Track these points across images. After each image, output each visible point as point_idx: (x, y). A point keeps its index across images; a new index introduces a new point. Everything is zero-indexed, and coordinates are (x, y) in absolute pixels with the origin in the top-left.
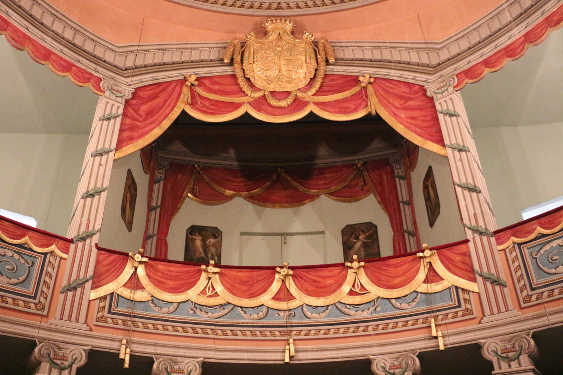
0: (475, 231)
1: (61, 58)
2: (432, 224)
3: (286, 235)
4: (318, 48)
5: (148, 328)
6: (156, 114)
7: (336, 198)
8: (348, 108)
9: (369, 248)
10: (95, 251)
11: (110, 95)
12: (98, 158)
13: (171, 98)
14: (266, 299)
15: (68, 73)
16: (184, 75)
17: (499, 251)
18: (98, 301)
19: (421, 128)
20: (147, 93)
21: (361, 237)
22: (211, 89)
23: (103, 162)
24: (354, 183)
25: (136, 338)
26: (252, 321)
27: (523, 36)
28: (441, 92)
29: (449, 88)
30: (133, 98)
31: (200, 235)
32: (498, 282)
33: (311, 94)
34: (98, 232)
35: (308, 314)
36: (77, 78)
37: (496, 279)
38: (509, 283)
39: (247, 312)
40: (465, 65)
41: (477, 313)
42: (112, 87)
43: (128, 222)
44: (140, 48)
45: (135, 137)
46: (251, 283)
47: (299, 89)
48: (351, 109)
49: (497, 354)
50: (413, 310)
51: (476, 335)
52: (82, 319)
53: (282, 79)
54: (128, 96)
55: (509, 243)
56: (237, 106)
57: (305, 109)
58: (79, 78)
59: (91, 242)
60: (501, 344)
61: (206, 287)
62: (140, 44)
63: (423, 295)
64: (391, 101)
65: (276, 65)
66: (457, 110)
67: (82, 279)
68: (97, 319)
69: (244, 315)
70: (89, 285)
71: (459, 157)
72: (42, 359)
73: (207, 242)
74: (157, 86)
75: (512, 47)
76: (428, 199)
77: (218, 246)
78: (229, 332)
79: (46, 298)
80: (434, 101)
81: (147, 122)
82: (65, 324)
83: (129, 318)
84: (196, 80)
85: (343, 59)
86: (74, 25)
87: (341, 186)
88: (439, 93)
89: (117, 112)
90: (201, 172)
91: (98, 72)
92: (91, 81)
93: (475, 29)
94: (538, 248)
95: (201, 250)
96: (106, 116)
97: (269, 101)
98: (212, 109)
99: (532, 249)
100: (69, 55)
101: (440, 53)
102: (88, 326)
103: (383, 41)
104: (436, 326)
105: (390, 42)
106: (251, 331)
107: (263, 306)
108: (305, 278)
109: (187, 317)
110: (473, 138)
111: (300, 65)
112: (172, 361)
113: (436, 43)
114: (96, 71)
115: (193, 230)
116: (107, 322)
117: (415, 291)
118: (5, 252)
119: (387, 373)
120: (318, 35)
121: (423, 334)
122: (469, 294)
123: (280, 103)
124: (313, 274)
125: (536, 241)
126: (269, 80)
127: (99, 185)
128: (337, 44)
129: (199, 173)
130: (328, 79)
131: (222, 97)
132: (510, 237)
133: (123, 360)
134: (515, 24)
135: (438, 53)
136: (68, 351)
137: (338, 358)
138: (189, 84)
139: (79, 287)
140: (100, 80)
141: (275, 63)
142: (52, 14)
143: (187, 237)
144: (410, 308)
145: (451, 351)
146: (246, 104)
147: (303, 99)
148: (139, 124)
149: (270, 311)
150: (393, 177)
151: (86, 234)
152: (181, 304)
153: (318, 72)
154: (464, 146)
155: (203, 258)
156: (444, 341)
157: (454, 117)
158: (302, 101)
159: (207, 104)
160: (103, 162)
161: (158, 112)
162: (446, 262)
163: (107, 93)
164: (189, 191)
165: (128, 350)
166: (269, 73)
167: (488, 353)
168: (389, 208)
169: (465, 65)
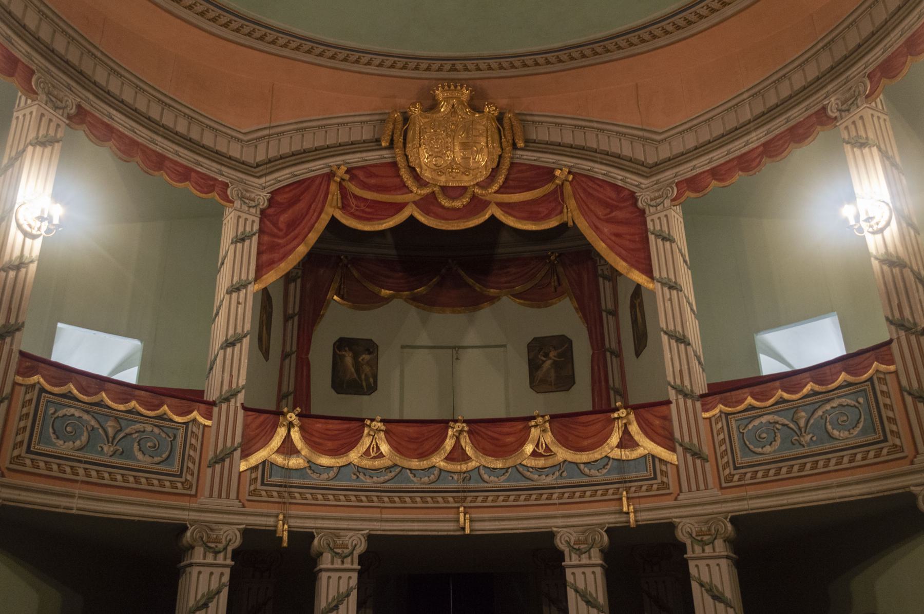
0: (680, 391)
1: (176, 163)
2: (638, 354)
5: (306, 499)
6: (299, 224)
7: (521, 301)
10: (241, 413)
11: (241, 208)
12: (234, 295)
14: (438, 460)
15: (187, 183)
16: (330, 166)
18: (249, 472)
20: (286, 196)
21: (552, 354)
26: (423, 486)
27: (761, 145)
28: (655, 204)
29: (665, 201)
30: (270, 206)
31: (350, 350)
32: (699, 456)
34: (243, 388)
35: (486, 477)
36: (198, 188)
37: (697, 451)
38: (712, 458)
39: (417, 475)
40: (688, 172)
41: (673, 488)
42: (242, 193)
47: (478, 183)
48: (542, 215)
51: (671, 513)
52: (233, 494)
53: (456, 169)
54: (263, 204)
55: (716, 411)
56: (400, 207)
57: (485, 212)
58: (201, 187)
59: (236, 402)
60: (696, 525)
63: (615, 461)
64: (592, 207)
65: (448, 151)
67: (230, 448)
68: (249, 492)
69: (413, 479)
70: (237, 454)
71: (668, 297)
73: (360, 359)
76: (634, 321)
77: (374, 364)
79: (192, 474)
81: (289, 237)
82: (215, 503)
84: (347, 172)
86: (187, 111)
87: (528, 286)
88: (652, 206)
90: (349, 266)
91: (224, 175)
92: (217, 189)
93: (705, 121)
95: (353, 370)
98: (369, 213)
99: (740, 422)
100: (186, 157)
101: (659, 149)
102: (240, 502)
103: (588, 118)
104: (628, 498)
106: (421, 497)
109: (349, 483)
110: (689, 268)
112: (335, 535)
113: (655, 133)
115: (342, 344)
116: (261, 496)
118: (144, 427)
119: (571, 548)
120: (503, 102)
121: (613, 507)
122: (666, 466)
123: (453, 204)
125: (746, 413)
126: (439, 170)
127: (239, 330)
128: (529, 118)
129: (347, 266)
132: (718, 404)
133: (281, 538)
134: (754, 125)
135: (657, 148)
136: (222, 532)
138: (338, 180)
140: (226, 185)
141: (447, 147)
144: (601, 476)
145: (642, 528)
146: (411, 204)
148: (280, 241)
151: (230, 394)
152: (342, 468)
153: (502, 161)
154: (676, 283)
157: (668, 242)
158: (482, 200)
161: (302, 222)
162: (644, 426)
163: (237, 204)
164: (334, 292)
165: (286, 527)
167: (683, 535)
169: (688, 172)
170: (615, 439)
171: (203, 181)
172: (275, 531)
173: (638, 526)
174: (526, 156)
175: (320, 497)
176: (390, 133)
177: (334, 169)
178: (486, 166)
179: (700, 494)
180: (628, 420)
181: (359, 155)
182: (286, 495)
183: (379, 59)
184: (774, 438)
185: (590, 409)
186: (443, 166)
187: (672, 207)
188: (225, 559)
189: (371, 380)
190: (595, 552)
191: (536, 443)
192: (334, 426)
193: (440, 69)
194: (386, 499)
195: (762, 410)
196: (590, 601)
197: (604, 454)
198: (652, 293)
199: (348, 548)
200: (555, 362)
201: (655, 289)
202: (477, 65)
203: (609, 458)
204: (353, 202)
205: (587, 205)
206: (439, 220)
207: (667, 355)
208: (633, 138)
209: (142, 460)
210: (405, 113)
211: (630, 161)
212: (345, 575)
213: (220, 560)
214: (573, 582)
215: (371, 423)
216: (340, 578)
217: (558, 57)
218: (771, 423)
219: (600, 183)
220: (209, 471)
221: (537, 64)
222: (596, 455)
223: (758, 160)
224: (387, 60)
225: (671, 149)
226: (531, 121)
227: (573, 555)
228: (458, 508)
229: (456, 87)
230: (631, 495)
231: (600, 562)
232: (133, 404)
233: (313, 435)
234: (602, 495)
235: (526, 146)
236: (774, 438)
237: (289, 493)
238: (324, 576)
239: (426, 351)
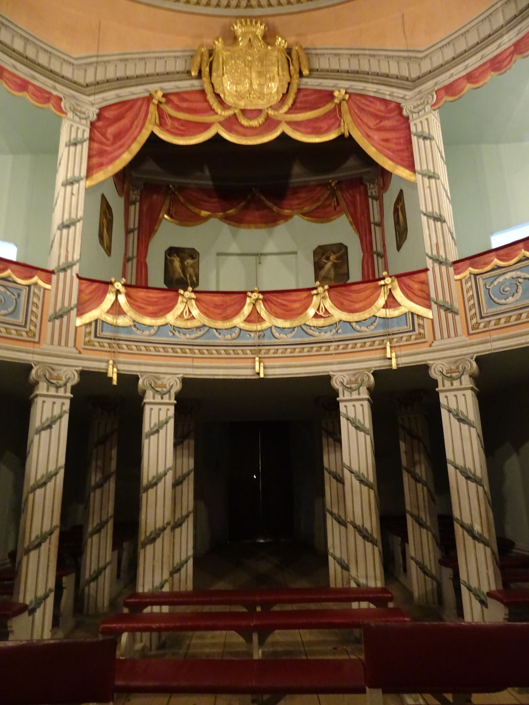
0: (437, 260)
1: (14, 75)
2: (399, 248)
3: (261, 256)
8: (321, 128)
10: (76, 281)
12: (69, 188)
14: (238, 321)
17: (456, 280)
19: (393, 151)
21: (332, 258)
23: (75, 192)
24: (327, 203)
25: (121, 358)
26: (227, 342)
27: (512, 45)
29: (426, 107)
31: (178, 256)
33: (283, 112)
34: (78, 261)
35: (277, 335)
37: (449, 307)
41: (429, 337)
43: (107, 247)
44: (100, 59)
48: (324, 129)
49: (442, 374)
55: (466, 274)
56: (207, 126)
59: (72, 272)
61: (183, 312)
64: (365, 120)
66: (431, 133)
70: (74, 312)
71: (428, 185)
73: (186, 263)
75: (500, 59)
76: (397, 223)
77: (196, 267)
78: (205, 352)
79: (35, 326)
82: (55, 349)
83: (113, 341)
86: (23, 34)
87: (314, 206)
88: (415, 113)
90: (176, 193)
92: (52, 101)
93: (462, 34)
95: (180, 271)
97: (240, 121)
101: (422, 65)
102: (77, 349)
104: (391, 347)
105: (369, 50)
106: (225, 350)
107: (236, 328)
108: (274, 302)
111: (271, 78)
113: (419, 51)
114: (55, 88)
115: (172, 251)
117: (374, 316)
119: (344, 387)
120: (292, 39)
121: (379, 354)
122: (423, 320)
126: (240, 96)
129: (174, 194)
130: (301, 94)
133: (111, 379)
135: (419, 65)
136: (62, 372)
137: (302, 373)
139: (65, 315)
140: (61, 99)
143: (166, 258)
145: (403, 370)
148: (108, 148)
149: (242, 332)
152: (161, 328)
153: (291, 86)
154: (434, 173)
155: (182, 278)
156: (397, 361)
159: (176, 124)
160: (74, 192)
163: (70, 115)
165: (115, 370)
166: (240, 88)
167: (435, 372)
168: (360, 229)
170: (382, 301)
172: (106, 373)
173: (399, 369)
177: (153, 93)
178: (277, 92)
179: (450, 340)
180: (393, 286)
184: (517, 290)
187: (432, 111)
188: (65, 392)
189: (194, 279)
191: (317, 307)
194: (197, 351)
195: (507, 268)
197: (372, 314)
198: (414, 185)
203: (376, 317)
204: (169, 122)
205: (361, 119)
207: (426, 232)
211: (397, 78)
212: (164, 408)
214: (345, 412)
216: (160, 409)
218: (513, 278)
219: (371, 99)
222: (365, 315)
227: (346, 392)
228: (254, 358)
230: (393, 345)
233: (136, 301)
235: (310, 74)
236: (517, 290)
237: (118, 344)
239: (236, 257)
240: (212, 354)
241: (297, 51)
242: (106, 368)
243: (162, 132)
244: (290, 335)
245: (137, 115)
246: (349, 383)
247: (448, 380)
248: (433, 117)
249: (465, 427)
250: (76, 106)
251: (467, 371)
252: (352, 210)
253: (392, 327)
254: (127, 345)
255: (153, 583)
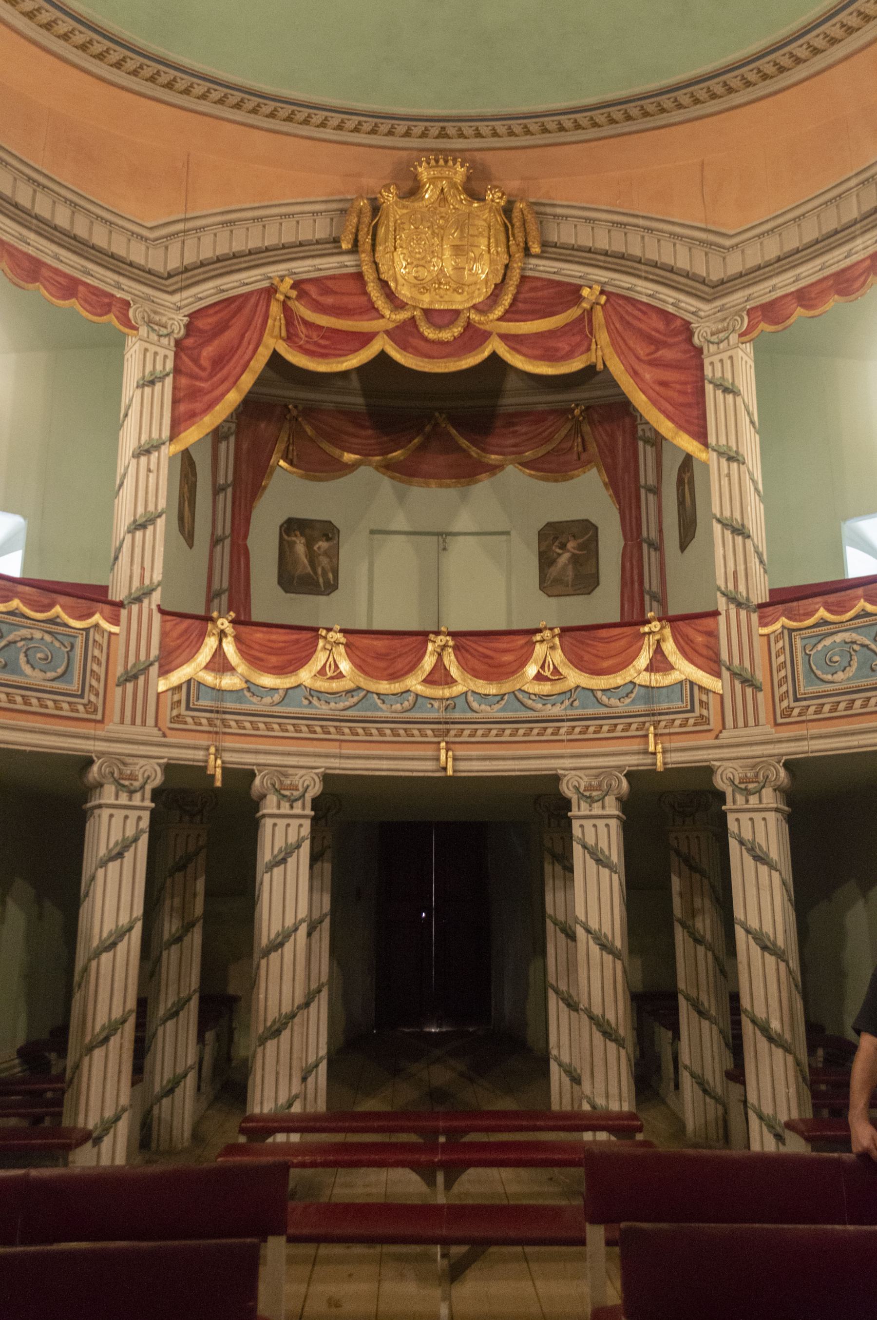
0: (732, 599)
1: (57, 271)
2: (683, 547)
4: (511, 222)
5: (244, 728)
6: (228, 362)
7: (532, 472)
8: (557, 350)
9: (581, 565)
10: (157, 617)
12: (143, 460)
13: (252, 327)
14: (414, 683)
15: (74, 300)
16: (270, 278)
17: (761, 635)
20: (210, 320)
21: (571, 545)
22: (317, 302)
23: (153, 466)
25: (229, 743)
26: (394, 715)
28: (716, 341)
30: (188, 335)
31: (302, 534)
33: (496, 317)
34: (158, 585)
35: (475, 705)
36: (89, 308)
37: (749, 677)
38: (767, 687)
40: (765, 294)
42: (149, 316)
44: (190, 225)
45: (197, 411)
46: (392, 657)
48: (563, 353)
49: (733, 783)
50: (626, 709)
53: (445, 285)
54: (179, 333)
55: (777, 626)
56: (366, 339)
57: (483, 347)
58: (94, 307)
60: (740, 770)
61: (325, 664)
62: (188, 216)
64: (631, 343)
65: (434, 257)
66: (736, 382)
67: (144, 662)
70: (154, 670)
71: (726, 471)
72: (104, 781)
73: (315, 548)
74: (225, 304)
76: (681, 503)
77: (334, 554)
79: (97, 695)
80: (703, 356)
81: (215, 379)
82: (127, 731)
84: (293, 287)
85: (555, 246)
86: (69, 195)
87: (542, 451)
88: (713, 343)
89: (164, 368)
90: (300, 419)
91: (123, 290)
92: (114, 309)
93: (794, 219)
94: (814, 641)
95: (306, 561)
96: (148, 378)
99: (806, 641)
101: (728, 259)
102: (160, 730)
103: (632, 212)
104: (656, 735)
106: (392, 729)
108: (472, 650)
110: (757, 432)
114: (119, 287)
116: (186, 723)
118: (32, 634)
120: (513, 185)
121: (636, 745)
123: (440, 335)
124: (485, 645)
125: (815, 630)
126: (421, 286)
127: (151, 508)
128: (549, 210)
129: (297, 420)
130: (527, 286)
131: (341, 321)
133: (213, 776)
135: (724, 259)
136: (138, 767)
137: (514, 770)
138: (282, 298)
140: (128, 304)
141: (433, 252)
142: (30, 178)
145: (670, 772)
147: (481, 327)
148: (202, 385)
149: (420, 700)
150: (634, 438)
151: (142, 592)
152: (290, 691)
153: (509, 274)
154: (737, 452)
155: (309, 574)
156: (664, 758)
158: (480, 329)
160: (153, 466)
161: (231, 358)
163: (143, 331)
164: (280, 455)
165: (219, 762)
166: (424, 273)
168: (621, 496)
169: (765, 294)
170: (643, 660)
171: (94, 297)
172: (206, 767)
174: (544, 266)
175: (262, 726)
176: (354, 230)
177: (276, 281)
178: (486, 281)
179: (748, 731)
180: (662, 635)
181: (309, 262)
182: (218, 723)
183: (335, 119)
184: (849, 662)
185: (617, 619)
186: (427, 280)
188: (143, 800)
189: (331, 576)
190: (610, 800)
192: (279, 636)
193: (424, 135)
194: (347, 731)
196: (601, 860)
197: (628, 679)
198: (706, 466)
199: (297, 790)
200: (574, 555)
201: (708, 460)
202: (477, 129)
203: (634, 684)
204: (302, 330)
205: (624, 341)
206: (419, 358)
207: (719, 551)
208: (692, 243)
209: (32, 676)
210: (376, 199)
211: (687, 276)
212: (295, 823)
213: (137, 800)
214: (580, 836)
215: (327, 634)
216: (288, 825)
217: (592, 119)
218: (846, 643)
219: (644, 308)
220: (119, 690)
221: (562, 129)
223: (862, 279)
224: (349, 120)
225: (744, 260)
226: (550, 215)
227: (583, 804)
228: (439, 743)
229: (446, 162)
230: (660, 731)
231: (617, 813)
232: (16, 603)
233: (251, 648)
234: (623, 730)
235: (543, 252)
236: (849, 662)
237: (223, 720)
238: (268, 823)
239: (403, 538)
240: (371, 735)
241: (521, 210)
242: (204, 758)
243: (290, 350)
244: (497, 707)
245: (249, 323)
246: (589, 788)
247: (741, 794)
248: (741, 353)
249: (763, 869)
250: (152, 315)
251: (770, 782)
252: (609, 460)
253: (659, 703)
254: (237, 721)
255: (276, 1098)
